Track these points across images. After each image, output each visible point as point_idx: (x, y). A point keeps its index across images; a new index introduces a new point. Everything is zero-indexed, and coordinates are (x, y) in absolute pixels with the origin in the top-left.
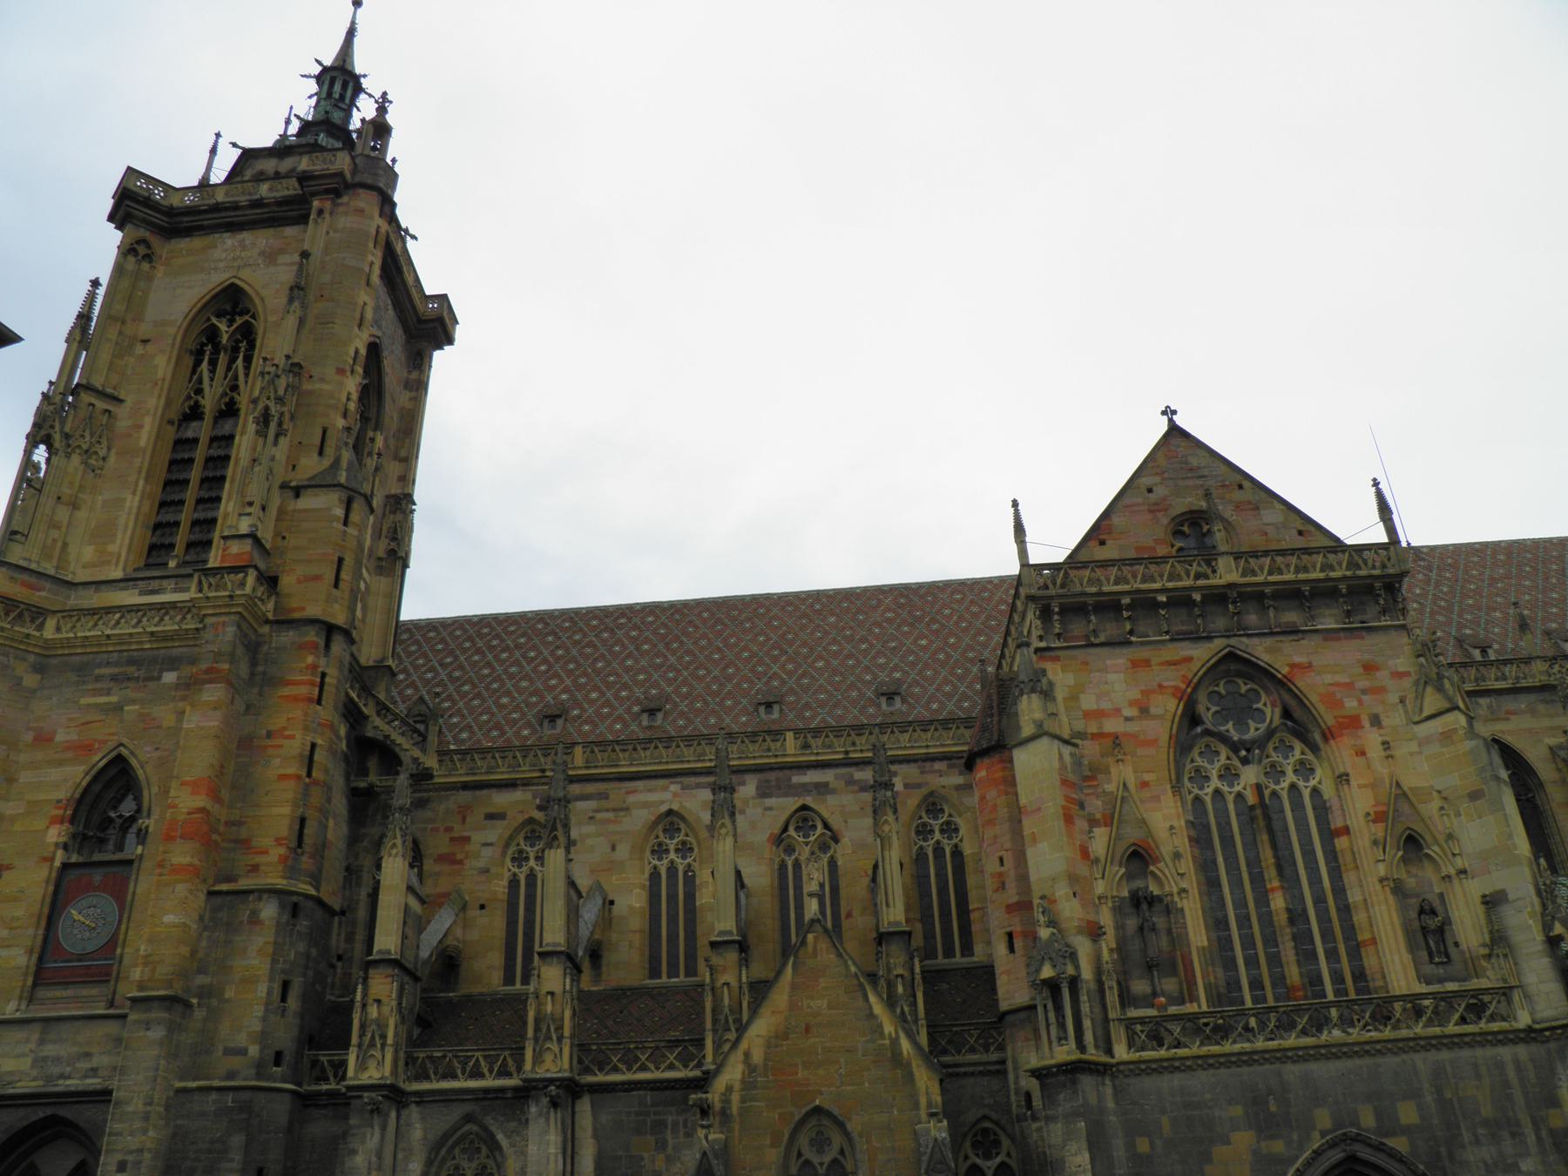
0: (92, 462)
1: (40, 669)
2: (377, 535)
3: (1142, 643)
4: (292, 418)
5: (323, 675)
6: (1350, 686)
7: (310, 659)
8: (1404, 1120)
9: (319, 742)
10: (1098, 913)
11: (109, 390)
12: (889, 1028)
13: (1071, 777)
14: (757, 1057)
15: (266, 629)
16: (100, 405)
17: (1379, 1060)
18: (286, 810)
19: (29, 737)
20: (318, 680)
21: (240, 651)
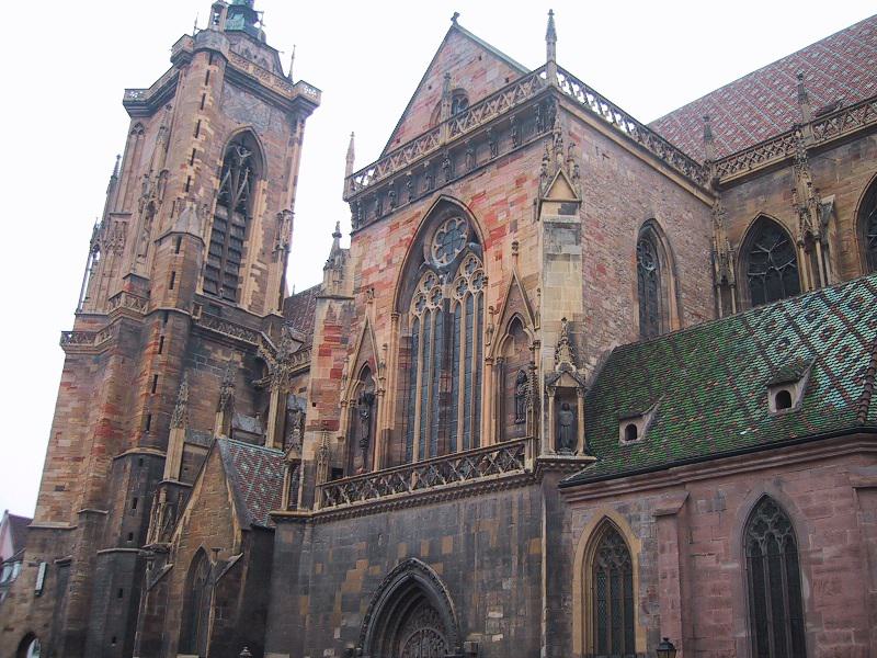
0: (119, 251)
1: (96, 362)
2: (267, 239)
3: (397, 211)
4: (161, 202)
5: (163, 338)
6: (503, 202)
7: (155, 332)
8: (443, 552)
9: (160, 373)
10: (339, 414)
11: (126, 211)
12: (230, 500)
13: (338, 323)
14: (188, 520)
15: (144, 321)
16: (120, 220)
17: (441, 506)
18: (140, 413)
19: (92, 396)
20: (159, 341)
21: (126, 336)
